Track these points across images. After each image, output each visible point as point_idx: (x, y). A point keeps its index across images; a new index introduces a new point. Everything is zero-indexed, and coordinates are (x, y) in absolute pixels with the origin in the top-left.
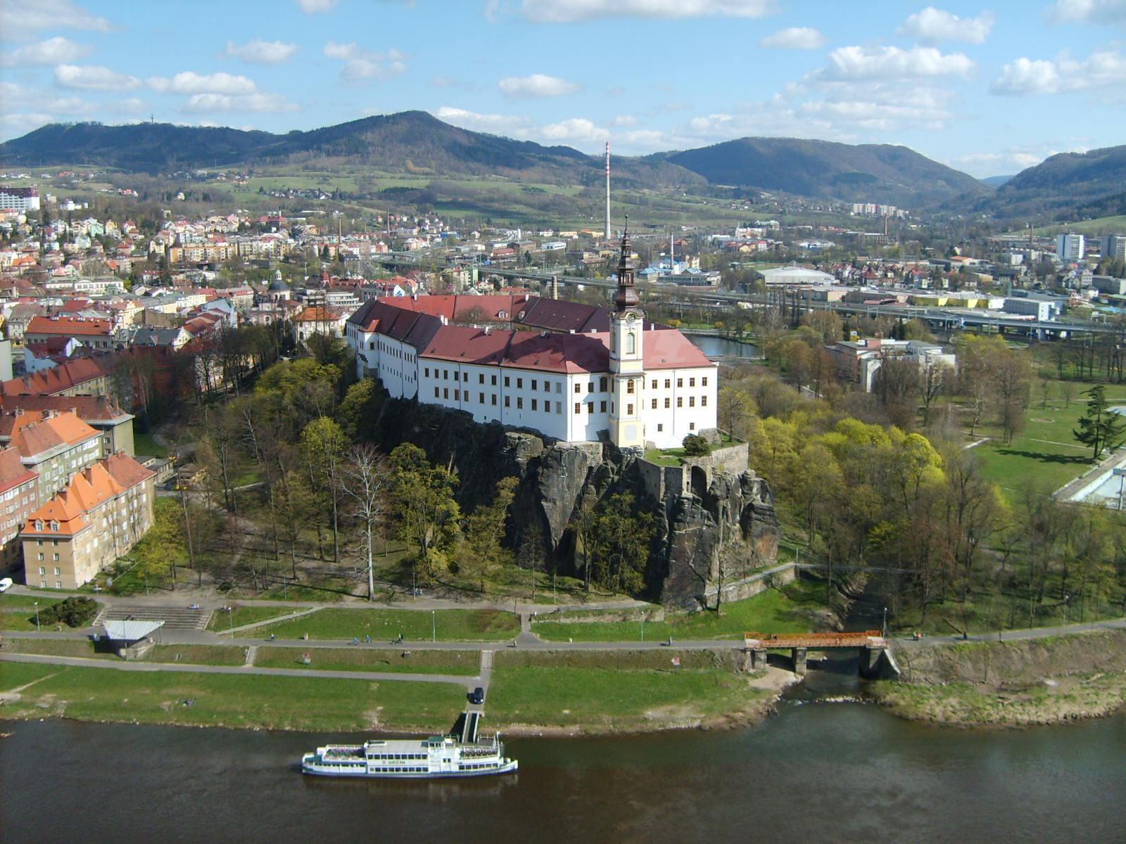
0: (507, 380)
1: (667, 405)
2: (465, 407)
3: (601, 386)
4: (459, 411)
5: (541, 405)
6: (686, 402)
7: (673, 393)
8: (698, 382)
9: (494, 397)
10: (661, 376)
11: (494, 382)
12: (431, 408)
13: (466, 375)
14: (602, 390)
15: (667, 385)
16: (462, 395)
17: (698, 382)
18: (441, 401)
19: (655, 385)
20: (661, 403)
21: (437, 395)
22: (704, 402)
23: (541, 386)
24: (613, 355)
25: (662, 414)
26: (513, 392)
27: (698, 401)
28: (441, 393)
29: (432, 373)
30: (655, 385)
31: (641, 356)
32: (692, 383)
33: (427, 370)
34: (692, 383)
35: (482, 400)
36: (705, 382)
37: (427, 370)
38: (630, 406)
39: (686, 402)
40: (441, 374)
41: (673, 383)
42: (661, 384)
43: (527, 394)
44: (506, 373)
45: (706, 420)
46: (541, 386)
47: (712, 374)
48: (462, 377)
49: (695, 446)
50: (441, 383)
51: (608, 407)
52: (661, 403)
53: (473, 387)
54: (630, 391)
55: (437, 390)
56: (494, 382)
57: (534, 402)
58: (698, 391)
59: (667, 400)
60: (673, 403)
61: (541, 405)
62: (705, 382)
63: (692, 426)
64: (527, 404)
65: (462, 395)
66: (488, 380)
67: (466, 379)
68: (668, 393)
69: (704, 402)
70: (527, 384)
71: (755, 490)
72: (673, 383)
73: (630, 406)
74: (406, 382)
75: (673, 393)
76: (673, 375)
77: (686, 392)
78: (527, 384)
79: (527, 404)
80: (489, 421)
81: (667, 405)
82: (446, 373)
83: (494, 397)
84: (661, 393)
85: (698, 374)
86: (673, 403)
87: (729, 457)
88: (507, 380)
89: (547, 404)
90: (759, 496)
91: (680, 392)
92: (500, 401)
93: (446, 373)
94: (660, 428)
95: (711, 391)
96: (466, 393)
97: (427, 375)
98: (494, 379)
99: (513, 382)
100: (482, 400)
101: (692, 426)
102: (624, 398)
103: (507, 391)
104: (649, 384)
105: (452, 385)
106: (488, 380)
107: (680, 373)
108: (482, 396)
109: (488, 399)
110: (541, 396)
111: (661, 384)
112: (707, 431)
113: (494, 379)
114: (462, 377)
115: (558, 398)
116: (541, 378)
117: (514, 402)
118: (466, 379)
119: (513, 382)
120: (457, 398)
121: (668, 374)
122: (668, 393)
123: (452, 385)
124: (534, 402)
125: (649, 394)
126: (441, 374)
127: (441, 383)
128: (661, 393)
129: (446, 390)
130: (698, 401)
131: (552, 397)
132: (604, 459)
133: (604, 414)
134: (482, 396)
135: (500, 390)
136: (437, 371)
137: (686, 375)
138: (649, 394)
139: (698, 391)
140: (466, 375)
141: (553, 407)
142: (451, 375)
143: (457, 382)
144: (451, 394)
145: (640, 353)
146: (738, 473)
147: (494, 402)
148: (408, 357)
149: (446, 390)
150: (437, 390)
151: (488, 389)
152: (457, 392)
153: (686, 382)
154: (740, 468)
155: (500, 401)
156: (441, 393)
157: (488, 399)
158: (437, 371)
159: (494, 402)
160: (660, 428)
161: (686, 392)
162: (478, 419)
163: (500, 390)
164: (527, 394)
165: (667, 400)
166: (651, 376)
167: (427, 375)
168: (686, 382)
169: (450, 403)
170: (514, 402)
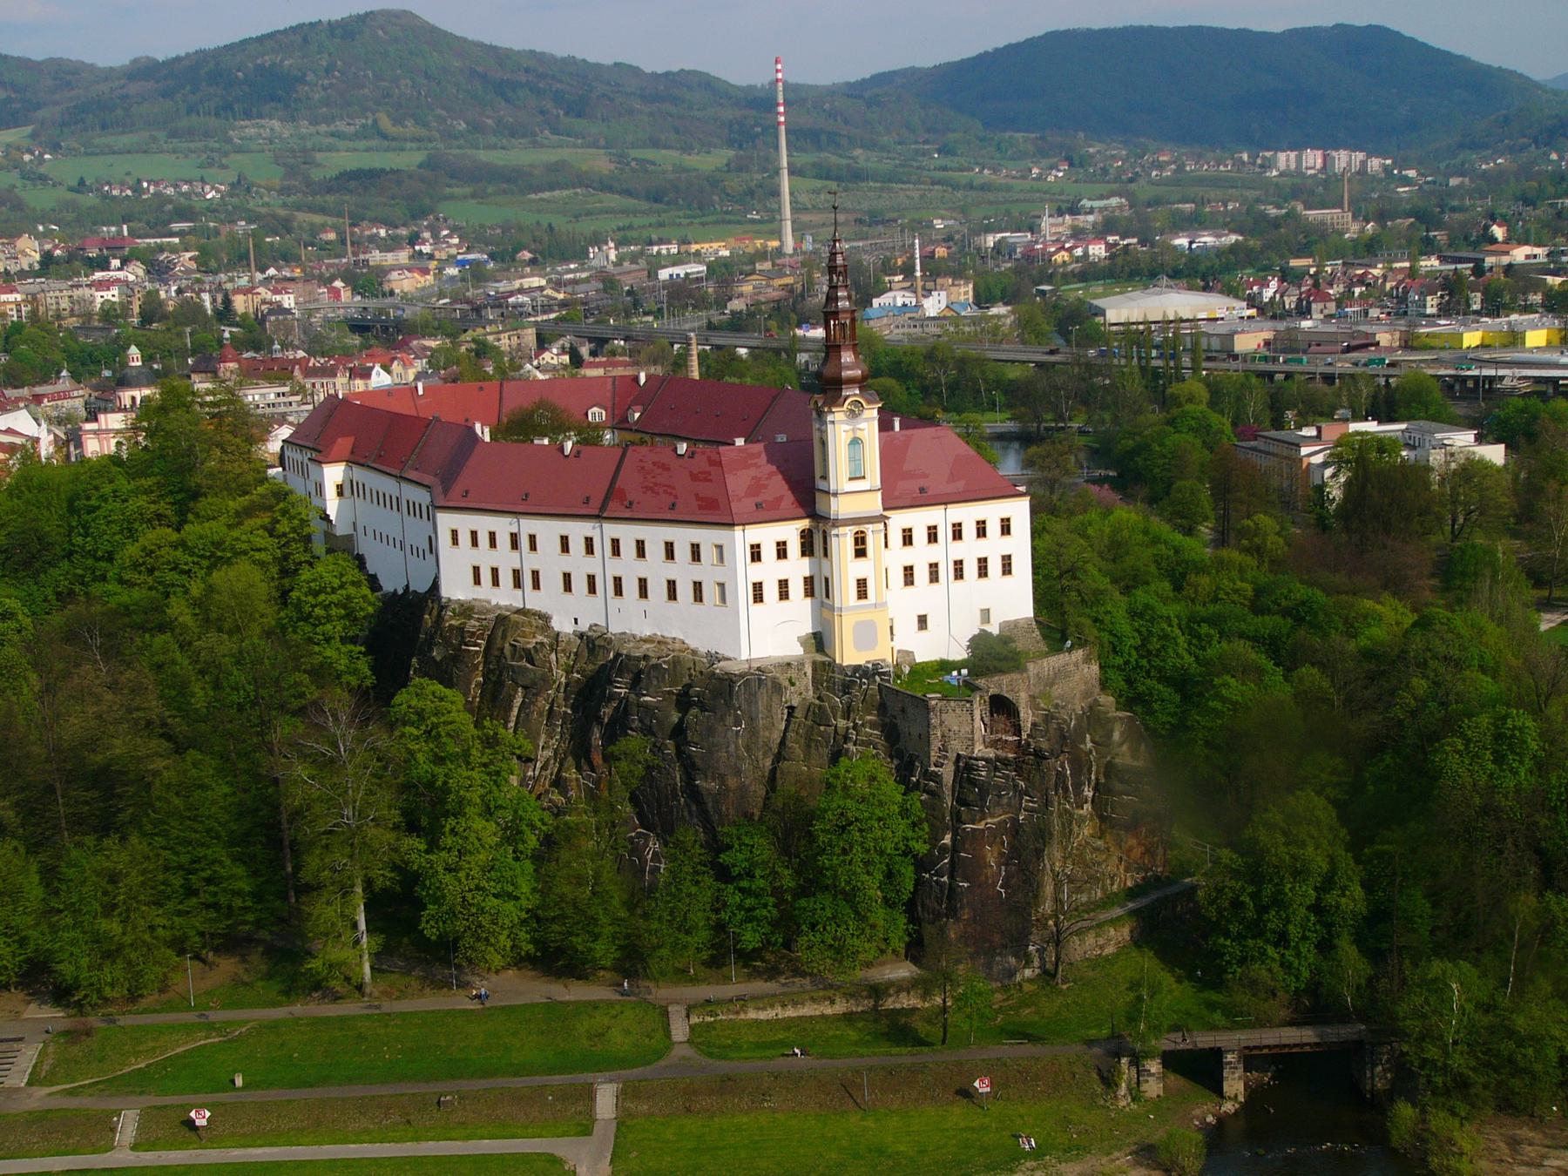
0: (616, 544)
1: (934, 577)
2: (535, 601)
3: (803, 545)
4: (522, 611)
5: (685, 591)
6: (971, 569)
7: (944, 553)
8: (993, 528)
9: (591, 580)
10: (919, 519)
11: (589, 548)
12: (466, 610)
13: (532, 538)
14: (803, 554)
15: (933, 536)
16: (527, 580)
17: (993, 528)
18: (485, 593)
19: (908, 539)
20: (921, 574)
21: (477, 581)
22: (1007, 568)
23: (683, 552)
24: (820, 484)
25: (924, 595)
26: (628, 567)
27: (995, 567)
28: (486, 576)
29: (465, 539)
30: (908, 539)
31: (878, 484)
32: (981, 531)
33: (454, 533)
35: (568, 587)
36: (1006, 528)
37: (454, 533)
38: (862, 585)
39: (971, 569)
40: (483, 539)
41: (944, 533)
42: (920, 536)
43: (656, 569)
44: (613, 530)
45: (1013, 600)
46: (683, 552)
47: (1019, 510)
48: (524, 543)
49: (991, 654)
50: (485, 558)
51: (819, 587)
52: (921, 574)
53: (549, 561)
54: (861, 553)
55: (476, 570)
56: (589, 548)
57: (672, 585)
58: (994, 546)
59: (934, 567)
61: (685, 591)
62: (1006, 528)
63: (986, 615)
64: (657, 590)
65: (527, 580)
66: (577, 545)
67: (533, 547)
68: (936, 553)
69: (1007, 568)
70: (655, 550)
71: (1116, 736)
72: (944, 533)
73: (862, 585)
74: (412, 559)
75: (944, 553)
77: (969, 551)
78: (655, 550)
79: (657, 590)
80: (584, 627)
81: (934, 577)
82: (492, 536)
83: (591, 580)
84: (921, 555)
85: (991, 512)
87: (1060, 674)
88: (616, 544)
89: (698, 586)
90: (1125, 748)
91: (958, 550)
92: (605, 586)
93: (492, 536)
94: (922, 621)
95: (1020, 545)
96: (535, 574)
97: (455, 541)
98: (589, 543)
99: (628, 549)
100: (568, 587)
101: (986, 615)
102: (846, 568)
103: (615, 567)
104: (896, 538)
105: (506, 559)
106: (577, 545)
108: (567, 578)
109: (580, 584)
110: (683, 572)
111: (920, 536)
112: (1016, 623)
113: (589, 543)
114: (524, 543)
115: (720, 574)
116: (683, 536)
117: (630, 587)
118: (533, 547)
119: (628, 549)
120: (518, 583)
122: (936, 553)
123: (506, 559)
124: (672, 585)
125: (899, 556)
126: (483, 539)
127: (485, 558)
128: (921, 555)
129: (495, 572)
130: (995, 567)
131: (707, 572)
132: (816, 688)
133: (809, 600)
134: (567, 578)
135: (603, 566)
136: (474, 534)
137: (966, 514)
138: (899, 556)
139: (994, 546)
140: (532, 538)
141: (710, 592)
142: (503, 541)
143: (516, 554)
144: (506, 578)
145: (874, 477)
146: (1079, 706)
147: (592, 589)
148: (414, 509)
149: (495, 572)
150: (476, 570)
151: (579, 564)
152: (517, 575)
153: (969, 530)
155: (605, 586)
156: (486, 576)
157: (580, 584)
158: (474, 534)
159: (592, 589)
160: (922, 621)
161: (969, 551)
162: (562, 624)
163: (603, 566)
164: (656, 569)
165: (934, 567)
166: (900, 520)
167: (455, 541)
168: (969, 530)
169: (505, 597)
170: (630, 587)
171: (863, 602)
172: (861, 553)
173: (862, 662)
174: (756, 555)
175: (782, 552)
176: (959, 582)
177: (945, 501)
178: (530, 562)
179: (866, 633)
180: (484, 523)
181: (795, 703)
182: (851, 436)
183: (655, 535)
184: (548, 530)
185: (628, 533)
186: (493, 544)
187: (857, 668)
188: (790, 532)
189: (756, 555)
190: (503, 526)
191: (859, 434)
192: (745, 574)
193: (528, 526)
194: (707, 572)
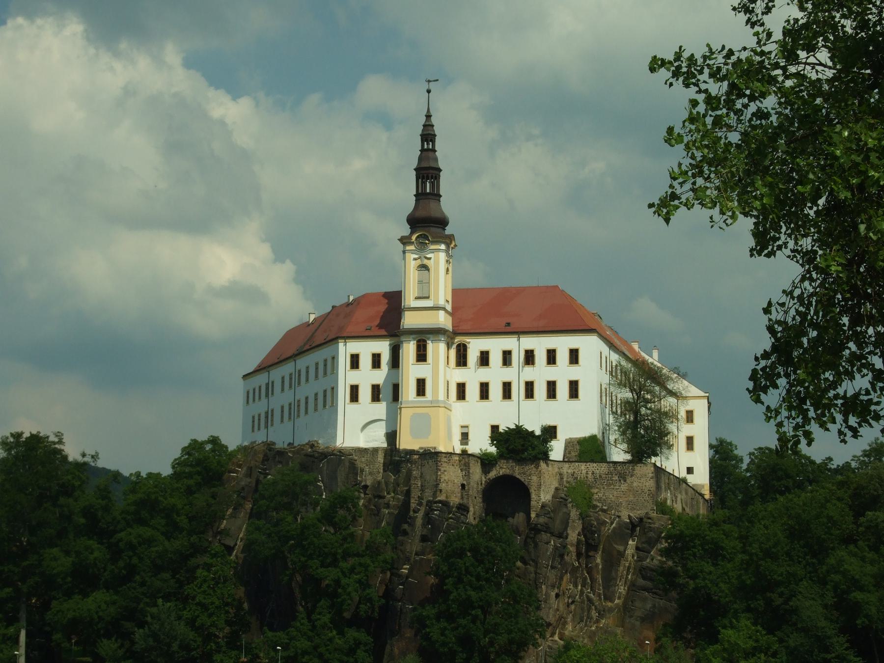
6: (540, 390)
7: (517, 374)
8: (563, 357)
10: (495, 345)
15: (507, 357)
17: (563, 357)
19: (484, 359)
20: (496, 391)
27: (563, 390)
34: (551, 356)
36: (574, 357)
39: (540, 390)
41: (518, 358)
42: (496, 358)
52: (496, 391)
54: (421, 357)
58: (563, 373)
60: (518, 390)
62: (574, 357)
72: (518, 358)
75: (517, 374)
76: (517, 345)
77: (540, 373)
85: (563, 344)
86: (518, 390)
91: (529, 373)
102: (412, 371)
107: (529, 342)
111: (496, 358)
121: (509, 343)
130: (563, 390)
137: (540, 344)
153: (541, 357)
154: (632, 506)
161: (540, 373)
168: (541, 357)
171: (421, 399)
172: (421, 357)
173: (416, 447)
174: (355, 361)
175: (376, 361)
176: (529, 402)
177: (519, 333)
179: (423, 425)
181: (369, 483)
182: (419, 262)
187: (412, 452)
188: (383, 347)
189: (355, 361)
191: (426, 262)
192: (346, 377)
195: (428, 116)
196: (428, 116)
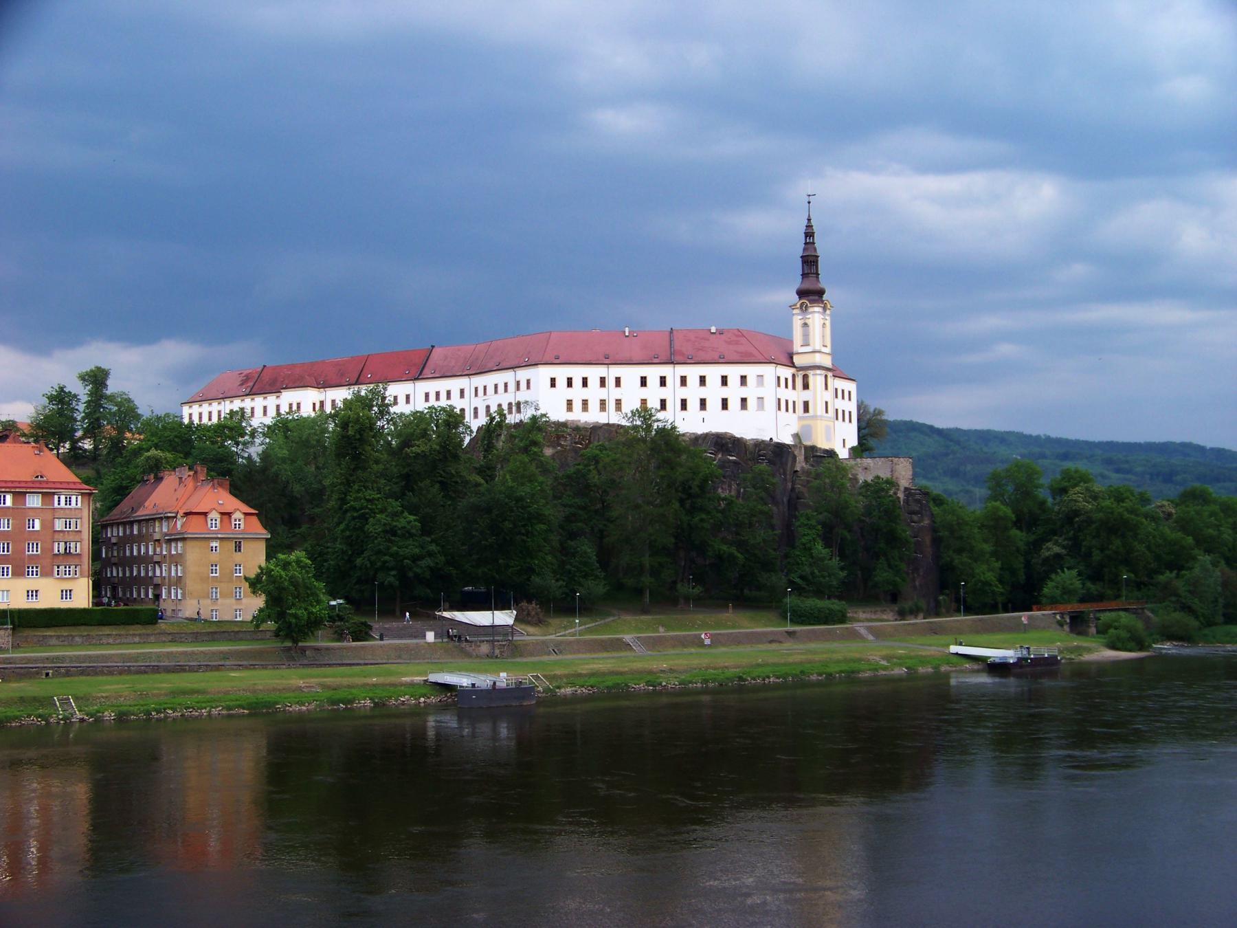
5: (734, 404)
44: (682, 370)
61: (734, 404)
79: (714, 404)
89: (744, 400)
110: (734, 392)
116: (733, 372)
131: (750, 392)
141: (751, 403)
150: (570, 403)
178: (612, 393)
180: (577, 372)
183: (714, 373)
184: (631, 374)
185: (693, 372)
186: (585, 382)
190: (594, 373)
193: (615, 371)
194: (750, 392)
195: (809, 220)
196: (809, 220)
